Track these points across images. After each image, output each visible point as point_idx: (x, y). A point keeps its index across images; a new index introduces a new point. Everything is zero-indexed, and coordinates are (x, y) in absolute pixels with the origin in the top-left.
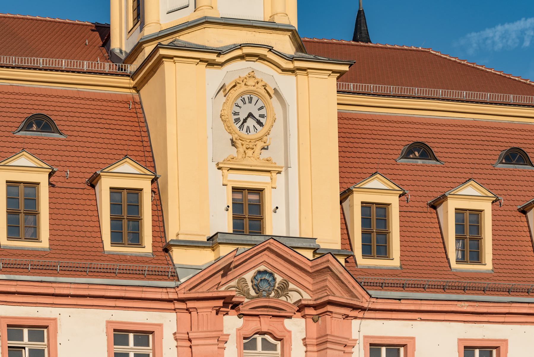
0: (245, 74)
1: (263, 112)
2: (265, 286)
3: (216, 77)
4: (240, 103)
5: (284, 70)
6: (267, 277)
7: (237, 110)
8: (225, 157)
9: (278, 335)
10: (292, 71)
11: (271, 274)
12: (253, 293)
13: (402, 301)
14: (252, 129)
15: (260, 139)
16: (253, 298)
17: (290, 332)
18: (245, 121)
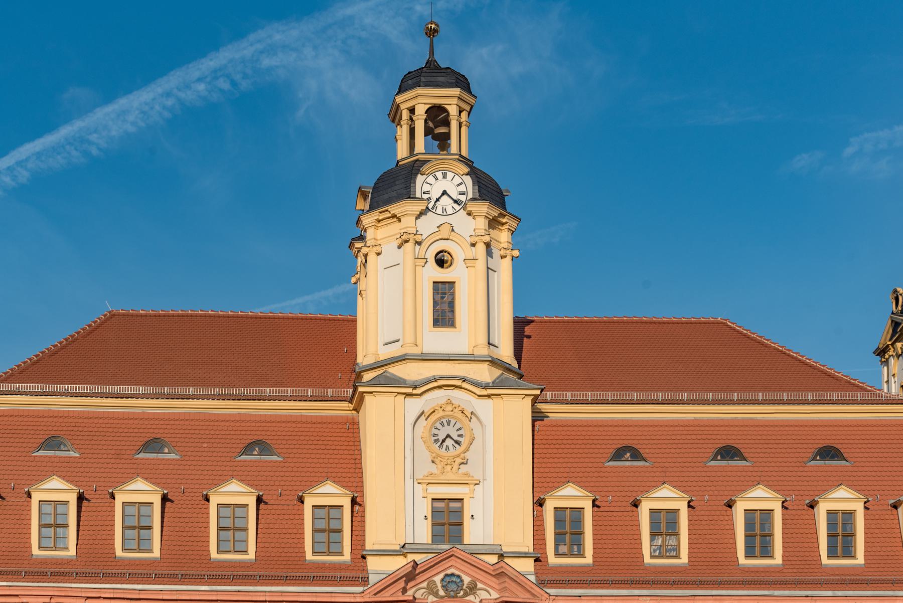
0: (444, 401)
1: (460, 432)
3: (415, 406)
4: (439, 426)
5: (479, 396)
6: (454, 579)
7: (436, 432)
8: (426, 474)
10: (489, 396)
11: (459, 576)
14: (451, 447)
15: (458, 456)
16: (442, 597)
18: (443, 441)
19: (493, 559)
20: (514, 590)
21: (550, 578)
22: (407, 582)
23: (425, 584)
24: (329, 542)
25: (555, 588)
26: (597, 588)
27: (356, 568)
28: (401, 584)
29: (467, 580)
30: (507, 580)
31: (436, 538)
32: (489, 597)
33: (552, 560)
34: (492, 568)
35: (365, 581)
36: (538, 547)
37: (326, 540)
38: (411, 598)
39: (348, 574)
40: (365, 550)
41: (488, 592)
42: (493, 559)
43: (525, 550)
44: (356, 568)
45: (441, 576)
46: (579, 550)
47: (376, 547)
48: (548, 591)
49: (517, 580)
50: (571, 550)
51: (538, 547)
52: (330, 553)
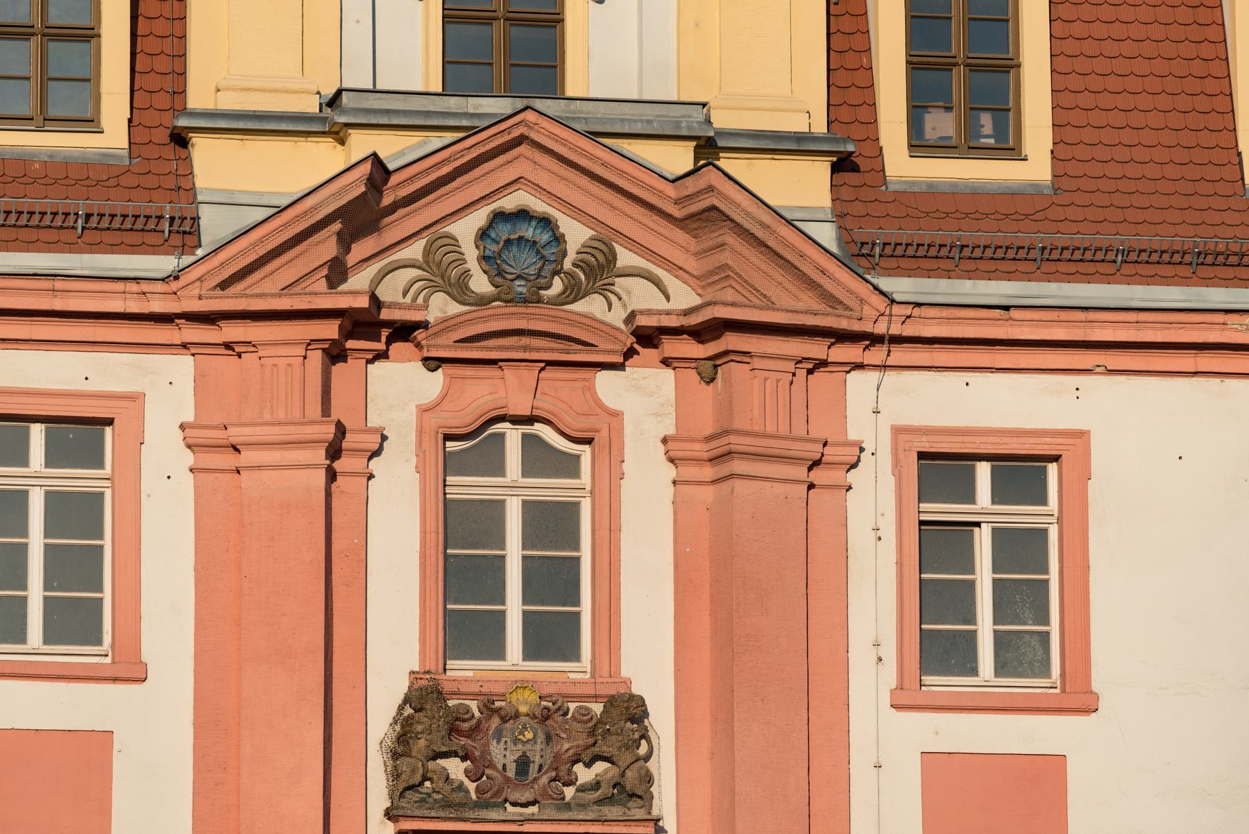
2: (525, 261)
6: (529, 232)
9: (576, 425)
11: (546, 222)
12: (480, 283)
13: (1014, 313)
16: (483, 301)
17: (617, 415)
19: (678, 158)
20: (757, 280)
21: (892, 233)
22: (345, 241)
23: (415, 250)
24: (46, 79)
25: (909, 273)
26: (1069, 277)
27: (151, 181)
28: (325, 247)
29: (576, 234)
30: (730, 239)
31: (460, 70)
32: (661, 304)
33: (901, 166)
34: (670, 190)
35: (184, 232)
36: (844, 114)
37: (32, 70)
38: (363, 302)
39: (119, 206)
40: (184, 111)
41: (658, 283)
42: (678, 158)
43: (797, 124)
44: (151, 181)
45: (479, 217)
46: (1000, 130)
47: (228, 102)
48: (886, 283)
49: (768, 236)
50: (970, 129)
51: (844, 114)
52: (46, 121)
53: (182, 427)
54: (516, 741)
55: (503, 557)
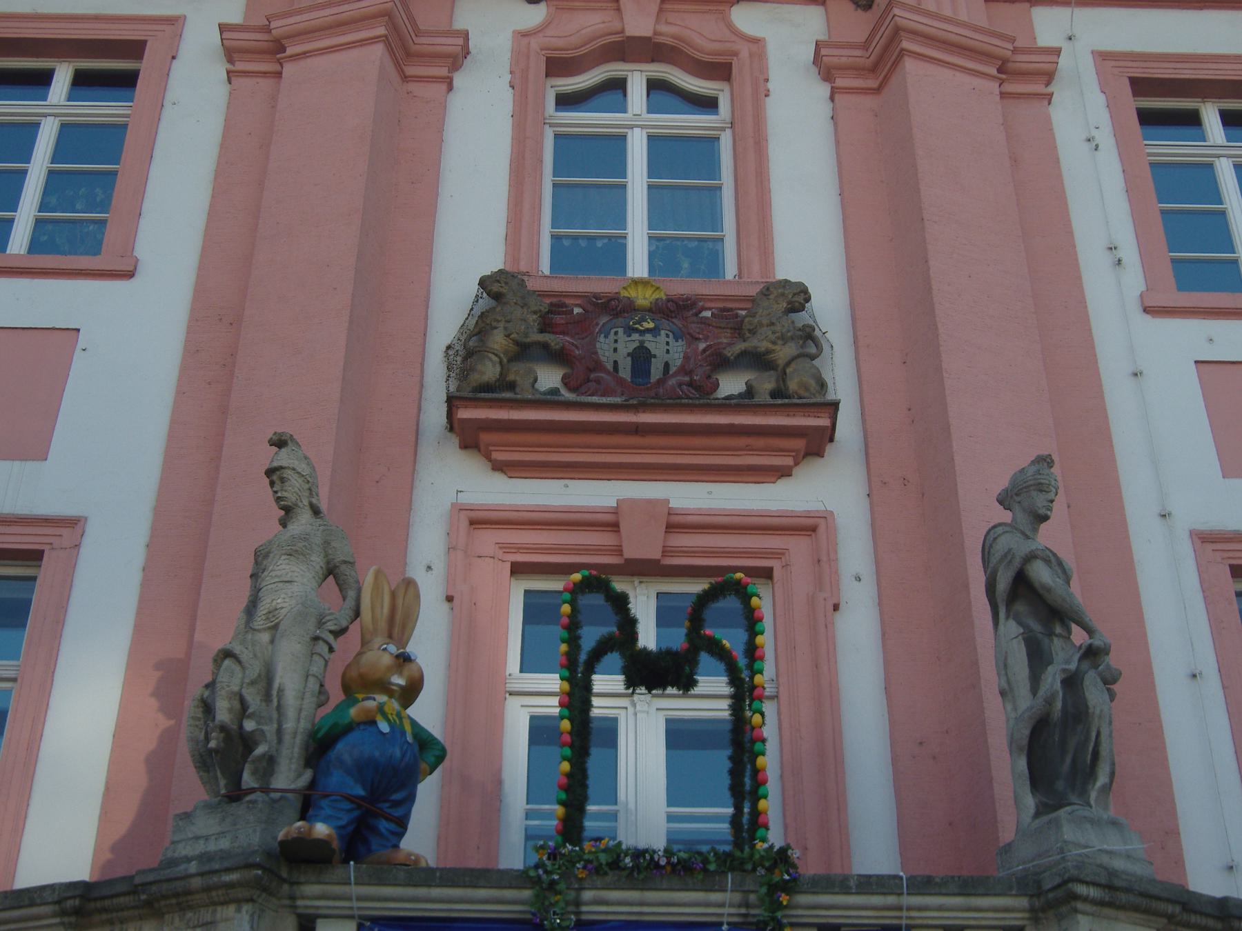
53: (223, 28)
54: (630, 330)
55: (624, 187)
